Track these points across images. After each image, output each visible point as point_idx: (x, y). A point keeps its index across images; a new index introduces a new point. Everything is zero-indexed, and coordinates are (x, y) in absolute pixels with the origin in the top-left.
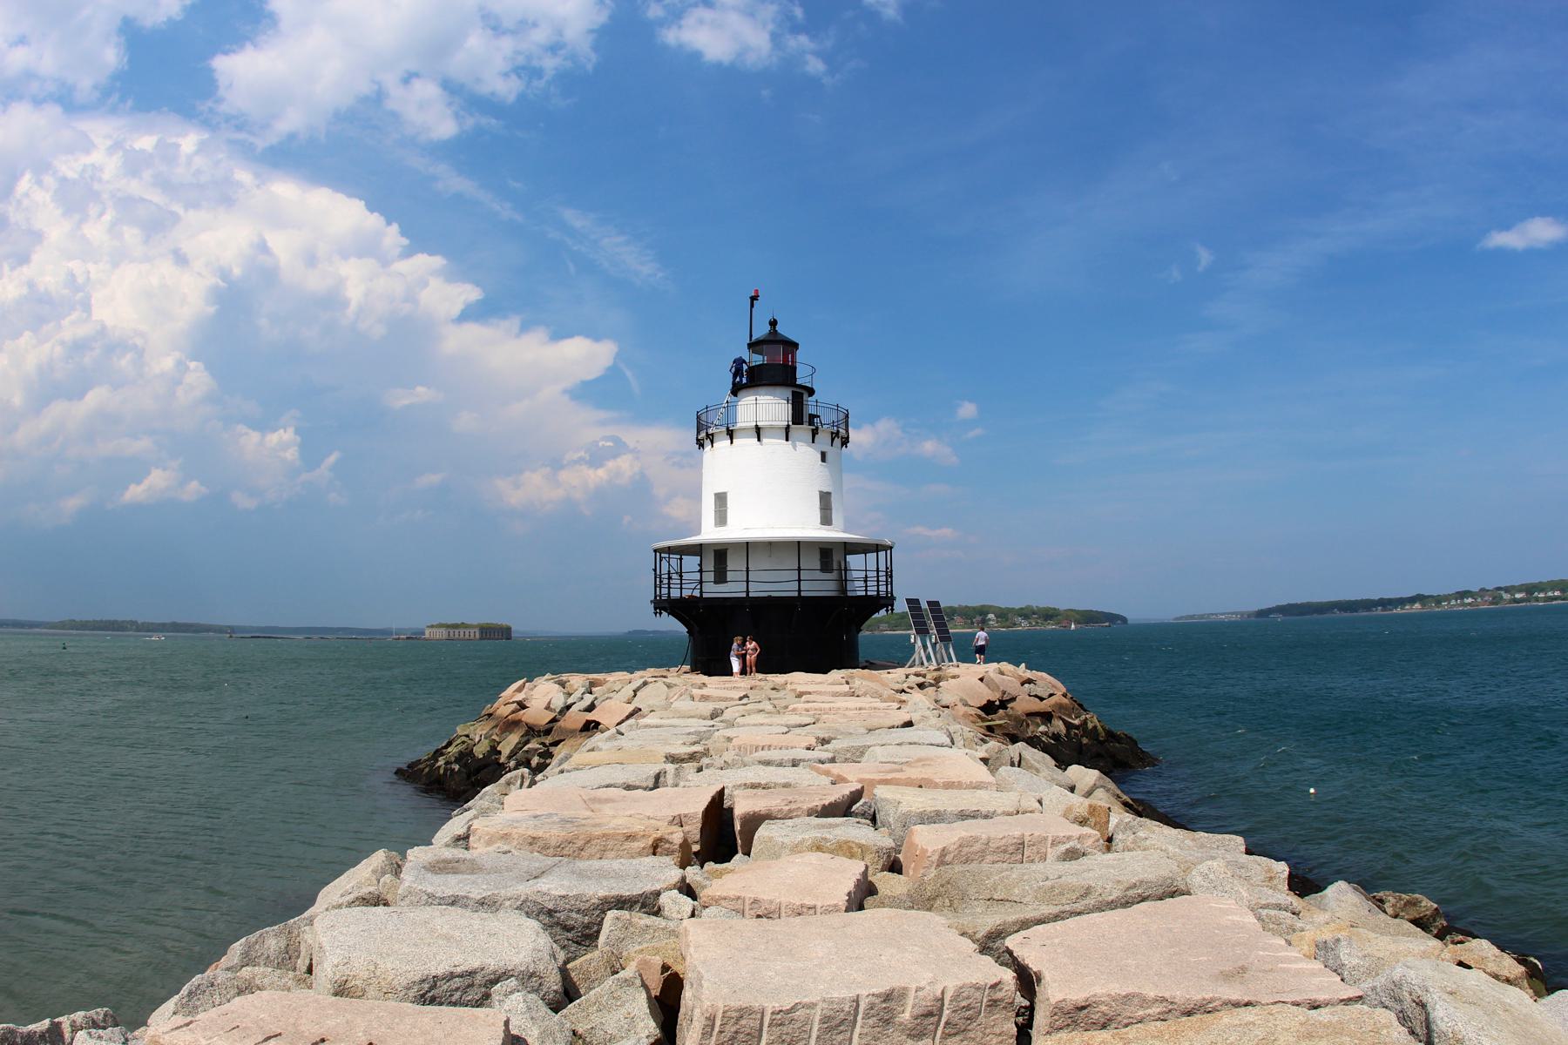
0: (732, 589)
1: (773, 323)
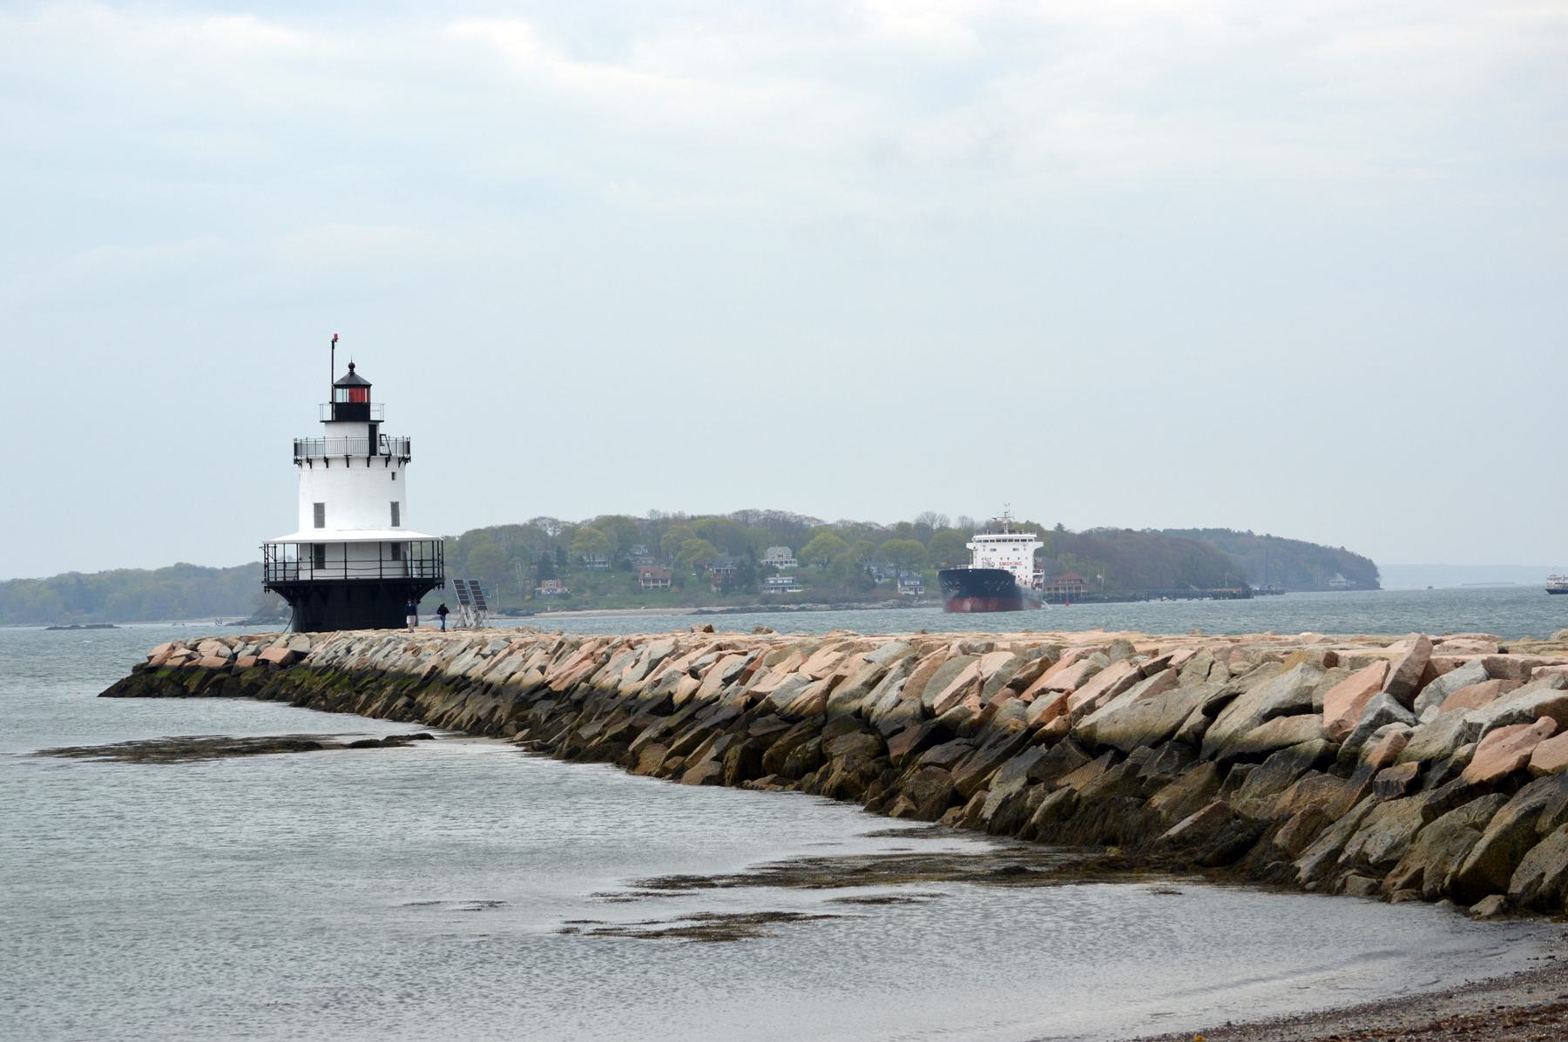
0: (331, 572)
1: (352, 366)
